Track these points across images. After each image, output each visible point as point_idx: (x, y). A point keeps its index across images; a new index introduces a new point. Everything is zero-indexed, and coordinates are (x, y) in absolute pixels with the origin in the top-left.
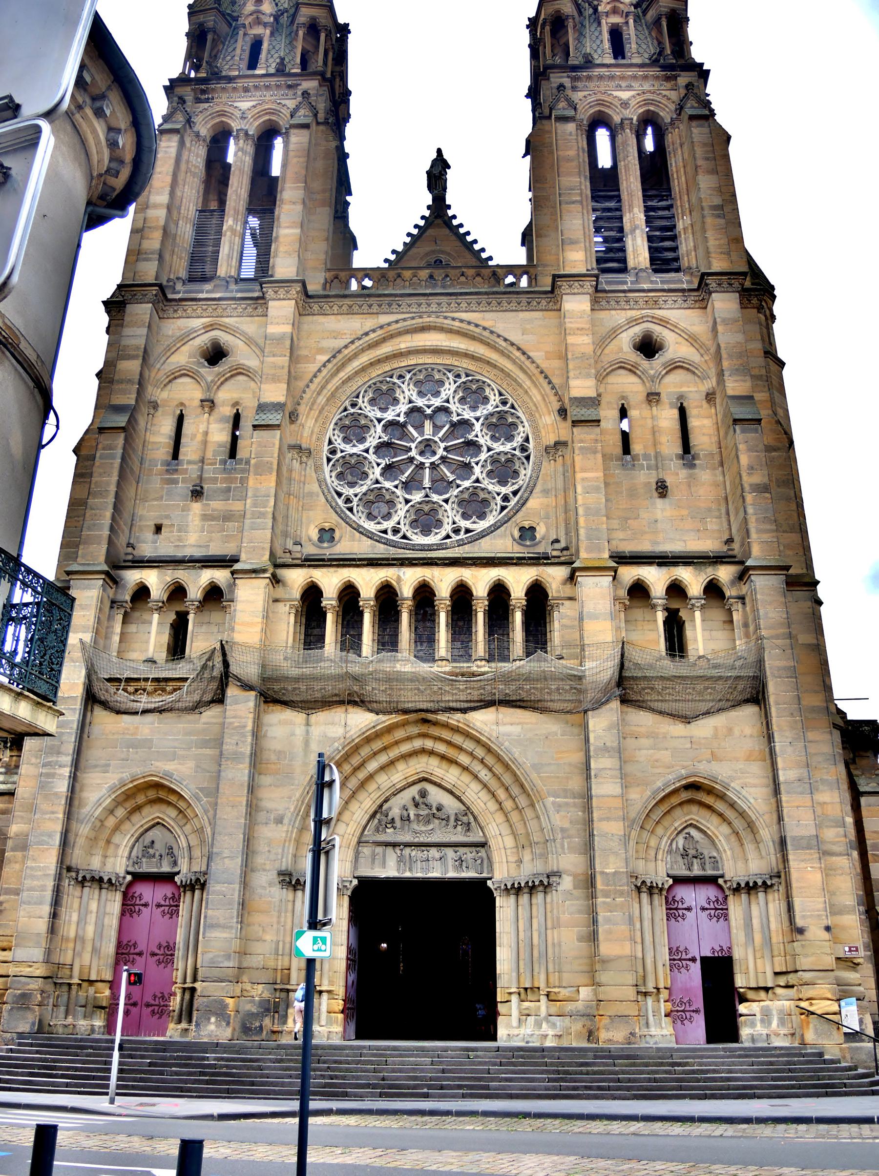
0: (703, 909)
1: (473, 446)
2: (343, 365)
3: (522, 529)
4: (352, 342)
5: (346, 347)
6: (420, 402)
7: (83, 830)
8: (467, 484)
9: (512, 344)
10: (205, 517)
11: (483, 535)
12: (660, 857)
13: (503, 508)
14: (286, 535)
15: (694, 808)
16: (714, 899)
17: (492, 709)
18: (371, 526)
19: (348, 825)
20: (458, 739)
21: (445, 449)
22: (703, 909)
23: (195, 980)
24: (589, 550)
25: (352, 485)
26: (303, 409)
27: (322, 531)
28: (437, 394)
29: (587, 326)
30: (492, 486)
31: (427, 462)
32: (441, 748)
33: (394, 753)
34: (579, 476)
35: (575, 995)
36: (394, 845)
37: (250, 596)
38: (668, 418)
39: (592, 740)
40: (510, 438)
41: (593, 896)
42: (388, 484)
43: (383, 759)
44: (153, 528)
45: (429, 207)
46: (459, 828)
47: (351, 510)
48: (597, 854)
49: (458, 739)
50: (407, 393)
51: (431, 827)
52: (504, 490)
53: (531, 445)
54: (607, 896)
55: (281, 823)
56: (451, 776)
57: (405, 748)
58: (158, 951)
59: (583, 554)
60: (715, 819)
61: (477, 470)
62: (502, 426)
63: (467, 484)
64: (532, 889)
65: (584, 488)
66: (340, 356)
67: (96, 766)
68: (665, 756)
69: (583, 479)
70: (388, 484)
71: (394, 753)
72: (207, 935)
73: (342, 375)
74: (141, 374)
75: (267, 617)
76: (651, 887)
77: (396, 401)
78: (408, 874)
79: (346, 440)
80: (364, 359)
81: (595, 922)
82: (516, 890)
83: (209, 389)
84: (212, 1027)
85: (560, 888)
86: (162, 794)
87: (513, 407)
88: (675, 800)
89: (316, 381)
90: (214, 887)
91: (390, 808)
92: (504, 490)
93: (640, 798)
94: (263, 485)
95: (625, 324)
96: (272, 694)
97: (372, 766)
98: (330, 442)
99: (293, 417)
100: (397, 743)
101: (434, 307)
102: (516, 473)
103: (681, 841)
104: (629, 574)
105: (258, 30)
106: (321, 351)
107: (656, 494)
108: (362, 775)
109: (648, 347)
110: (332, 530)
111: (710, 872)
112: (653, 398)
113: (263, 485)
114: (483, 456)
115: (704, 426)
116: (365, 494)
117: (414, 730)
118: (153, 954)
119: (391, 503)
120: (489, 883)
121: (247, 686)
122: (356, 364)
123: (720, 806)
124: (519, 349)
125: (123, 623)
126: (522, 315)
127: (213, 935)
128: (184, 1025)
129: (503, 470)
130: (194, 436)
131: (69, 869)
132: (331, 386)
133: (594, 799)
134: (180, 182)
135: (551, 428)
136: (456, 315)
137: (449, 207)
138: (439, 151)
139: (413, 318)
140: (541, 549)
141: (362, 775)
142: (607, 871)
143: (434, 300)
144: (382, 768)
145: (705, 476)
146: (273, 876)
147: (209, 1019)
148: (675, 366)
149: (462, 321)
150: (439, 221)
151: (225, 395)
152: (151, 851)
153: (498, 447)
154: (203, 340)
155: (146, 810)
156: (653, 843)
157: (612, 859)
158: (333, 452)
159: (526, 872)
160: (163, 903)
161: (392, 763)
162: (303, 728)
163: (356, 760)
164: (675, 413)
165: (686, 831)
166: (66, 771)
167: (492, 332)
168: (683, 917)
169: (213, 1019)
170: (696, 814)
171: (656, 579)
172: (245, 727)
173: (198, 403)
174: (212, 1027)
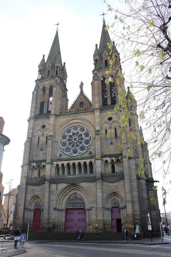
1: (82, 138)
2: (62, 127)
3: (90, 152)
4: (63, 123)
5: (62, 124)
6: (74, 132)
7: (27, 203)
8: (81, 145)
9: (88, 121)
10: (43, 154)
11: (83, 154)
13: (87, 149)
14: (54, 156)
15: (115, 196)
17: (83, 182)
18: (67, 153)
20: (79, 187)
21: (78, 139)
24: (97, 156)
25: (64, 146)
26: (56, 135)
27: (60, 154)
28: (77, 130)
29: (98, 117)
30: (85, 145)
31: (75, 142)
32: (77, 188)
33: (70, 189)
34: (96, 144)
37: (48, 167)
38: (113, 130)
40: (88, 137)
42: (69, 146)
43: (69, 190)
44: (36, 156)
45: (80, 92)
47: (64, 151)
49: (79, 187)
50: (72, 130)
51: (77, 200)
52: (87, 146)
53: (91, 138)
56: (79, 192)
57: (72, 189)
59: (97, 157)
60: (118, 198)
61: (83, 142)
62: (87, 135)
63: (81, 145)
65: (97, 146)
66: (62, 125)
67: (28, 193)
68: (110, 188)
69: (97, 144)
70: (69, 146)
73: (62, 128)
74: (32, 132)
75: (51, 170)
77: (71, 132)
78: (73, 208)
79: (63, 139)
80: (65, 125)
83: (43, 133)
87: (89, 131)
89: (58, 130)
91: (71, 198)
92: (87, 146)
93: (105, 195)
94: (49, 149)
96: (52, 181)
97: (67, 192)
98: (61, 140)
99: (55, 137)
101: (76, 116)
102: (89, 143)
103: (113, 201)
104: (105, 159)
105: (49, 69)
106: (59, 125)
107: (111, 144)
110: (61, 154)
111: (118, 206)
112: (110, 128)
113: (49, 149)
114: (84, 140)
116: (66, 148)
119: (70, 149)
121: (48, 181)
122: (64, 126)
123: (119, 196)
124: (89, 121)
125: (32, 171)
126: (89, 115)
129: (87, 142)
130: (41, 140)
131: (26, 208)
132: (60, 131)
134: (37, 98)
136: (79, 116)
137: (83, 92)
138: (81, 81)
139: (72, 118)
140: (92, 155)
143: (76, 114)
144: (69, 192)
146: (52, 209)
148: (114, 122)
149: (80, 118)
150: (82, 94)
151: (45, 133)
152: (37, 205)
153: (86, 138)
154: (42, 124)
155: (36, 199)
157: (100, 205)
158: (61, 141)
161: (70, 191)
163: (64, 191)
164: (114, 130)
166: (24, 195)
167: (85, 119)
170: (115, 197)
171: (109, 159)
173: (41, 135)
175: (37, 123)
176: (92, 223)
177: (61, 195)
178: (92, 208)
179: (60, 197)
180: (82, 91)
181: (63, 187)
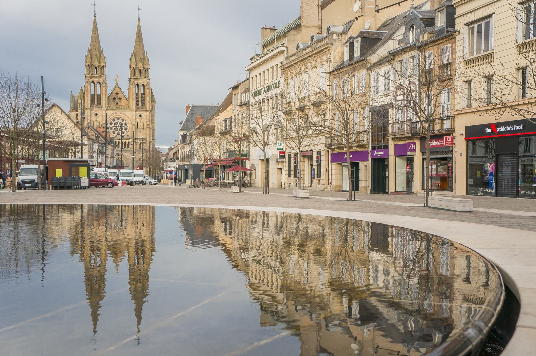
62: (126, 124)
95: (138, 113)
109: (140, 116)
115: (145, 125)
129: (126, 129)
135: (131, 126)
145: (145, 130)
159: (127, 165)
175: (92, 111)
180: (117, 84)
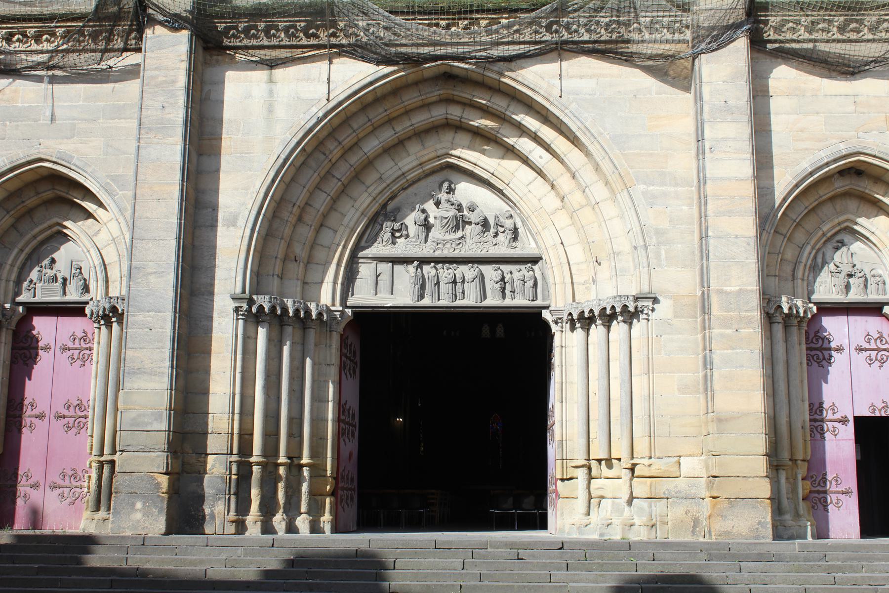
0: (860, 349)
12: (799, 274)
16: (876, 336)
19: (336, 232)
22: (860, 349)
23: (114, 452)
33: (403, 127)
35: (674, 470)
36: (405, 261)
39: (706, 97)
41: (706, 326)
43: (387, 136)
46: (501, 237)
48: (712, 265)
51: (460, 234)
54: (727, 326)
55: (234, 224)
57: (420, 119)
58: (66, 413)
64: (608, 318)
71: (403, 127)
72: (127, 385)
76: (789, 316)
81: (707, 363)
82: (586, 321)
84: (138, 516)
85: (653, 316)
86: (61, 191)
88: (825, 192)
90: (134, 318)
97: (372, 146)
100: (407, 113)
108: (355, 159)
111: (873, 296)
117: (435, 93)
118: (60, 417)
120: (546, 314)
121: (174, 22)
127: (136, 386)
128: (102, 514)
133: (709, 182)
141: (355, 159)
142: (728, 289)
147: (133, 505)
156: (789, 255)
160: (70, 345)
162: (264, 86)
165: (838, 238)
168: (829, 360)
169: (139, 505)
172: (174, 82)
174: (138, 516)
176: (641, 447)
177: (310, 178)
178: (640, 304)
179: (299, 195)
181: (340, 92)
